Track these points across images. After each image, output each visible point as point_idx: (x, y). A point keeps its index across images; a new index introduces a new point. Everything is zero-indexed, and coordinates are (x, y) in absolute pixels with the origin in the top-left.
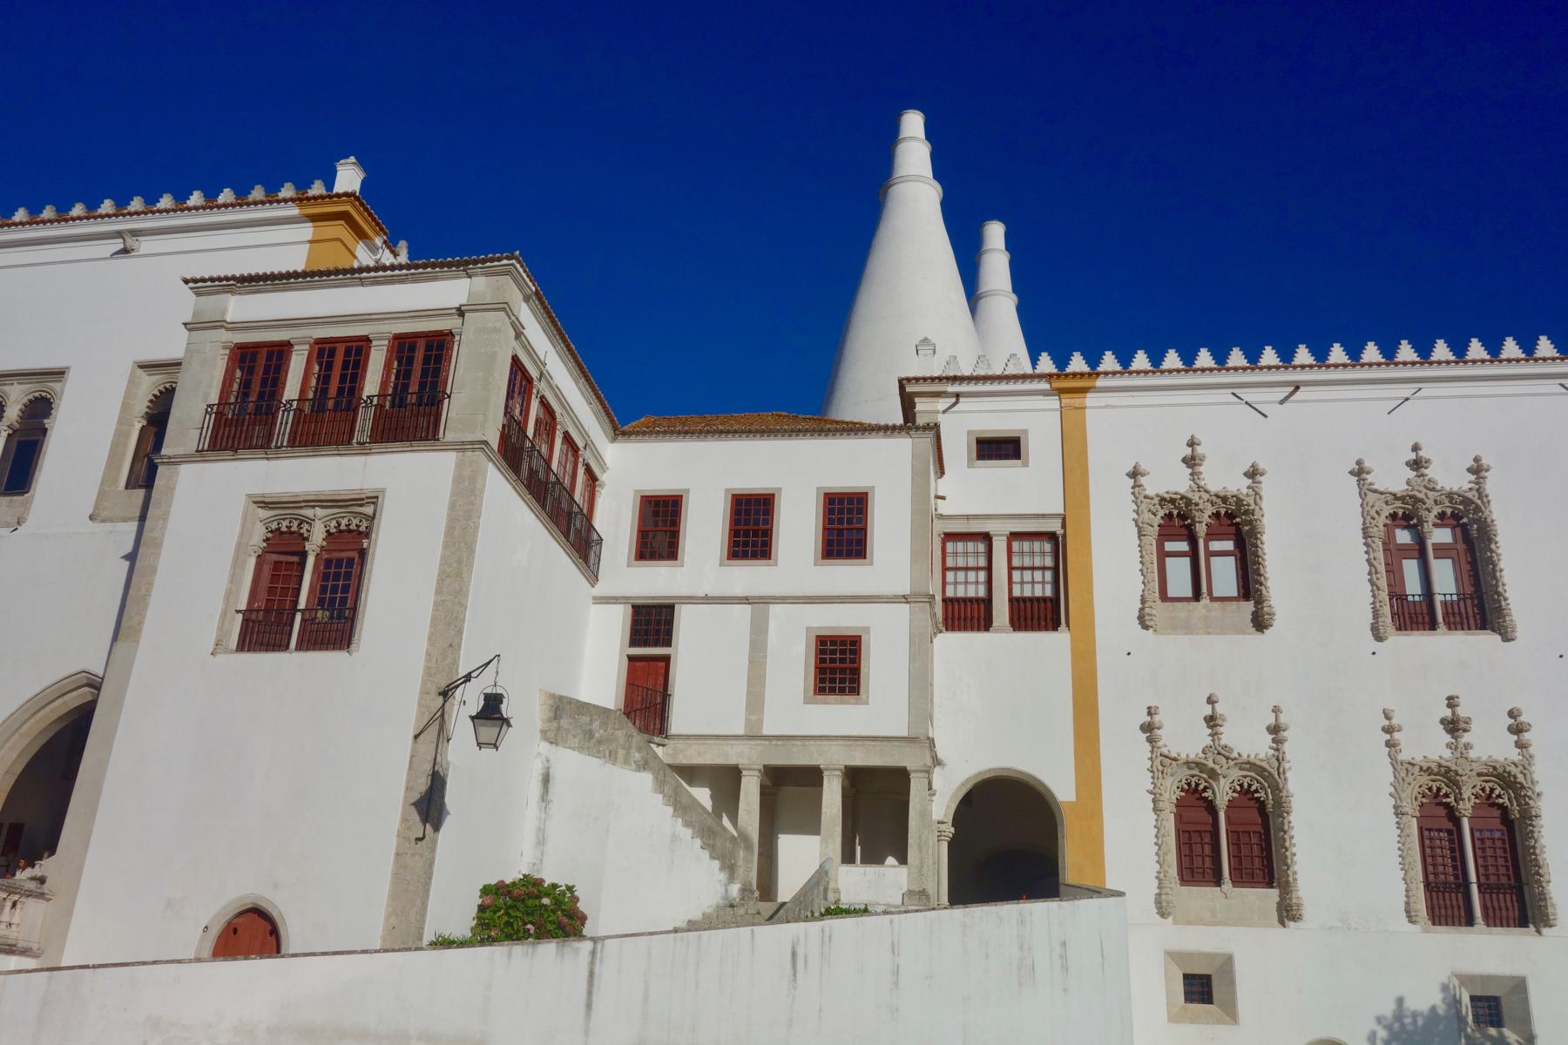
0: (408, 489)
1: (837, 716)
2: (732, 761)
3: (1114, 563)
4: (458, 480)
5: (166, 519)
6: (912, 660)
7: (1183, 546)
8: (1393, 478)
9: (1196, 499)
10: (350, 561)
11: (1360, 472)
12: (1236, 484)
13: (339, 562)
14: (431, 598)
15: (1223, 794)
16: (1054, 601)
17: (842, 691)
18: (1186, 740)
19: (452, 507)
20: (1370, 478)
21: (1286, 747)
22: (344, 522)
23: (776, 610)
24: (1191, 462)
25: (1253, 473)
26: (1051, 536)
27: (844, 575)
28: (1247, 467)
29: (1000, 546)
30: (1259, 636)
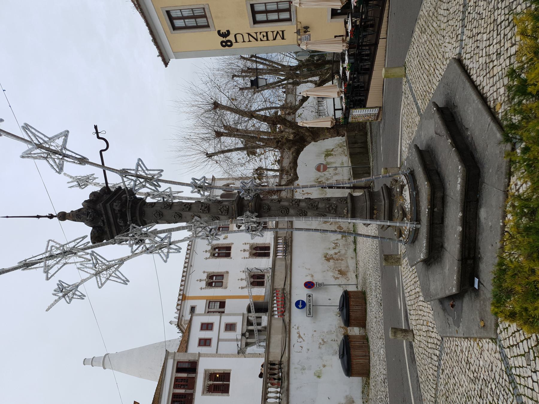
0: (205, 365)
3: (216, 292)
4: (204, 356)
7: (214, 284)
8: (208, 255)
9: (207, 280)
11: (206, 259)
12: (206, 275)
14: (224, 358)
15: (252, 280)
16: (221, 302)
18: (244, 283)
23: (220, 338)
24: (201, 280)
25: (204, 272)
26: (209, 302)
27: (216, 327)
29: (210, 310)
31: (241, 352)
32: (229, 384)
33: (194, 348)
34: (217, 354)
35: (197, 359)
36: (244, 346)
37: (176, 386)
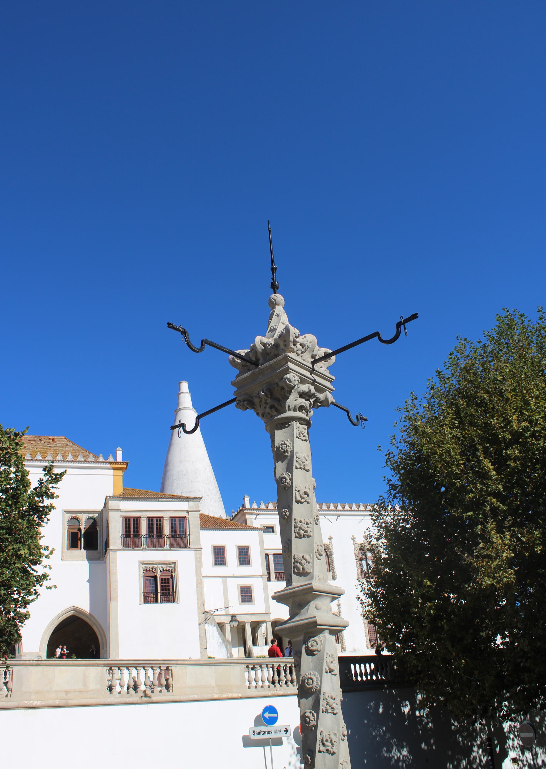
1: (247, 608)
2: (222, 621)
4: (196, 558)
5: (116, 567)
6: (264, 592)
10: (168, 579)
11: (353, 539)
13: (165, 579)
17: (248, 601)
19: (196, 565)
20: (355, 540)
21: (341, 609)
22: (165, 569)
25: (330, 539)
27: (245, 570)
28: (329, 537)
30: (333, 581)
31: (207, 616)
32: (156, 601)
33: (209, 539)
34: (200, 578)
35: (192, 547)
36: (219, 620)
37: (150, 520)
